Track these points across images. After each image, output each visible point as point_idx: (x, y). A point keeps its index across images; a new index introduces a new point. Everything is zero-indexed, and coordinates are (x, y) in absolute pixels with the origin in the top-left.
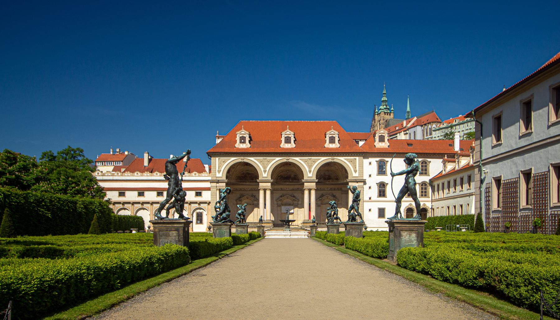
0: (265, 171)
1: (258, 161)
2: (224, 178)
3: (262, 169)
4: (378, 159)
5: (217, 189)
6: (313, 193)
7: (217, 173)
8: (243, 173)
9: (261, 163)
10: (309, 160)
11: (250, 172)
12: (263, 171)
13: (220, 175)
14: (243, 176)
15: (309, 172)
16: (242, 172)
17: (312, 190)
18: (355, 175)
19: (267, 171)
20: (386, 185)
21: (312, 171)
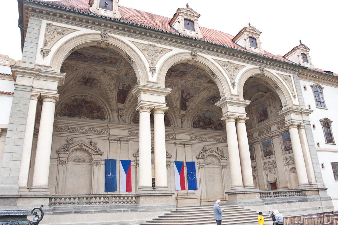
0: (153, 70)
1: (139, 47)
2: (57, 68)
3: (147, 66)
4: (313, 83)
5: (32, 96)
6: (242, 126)
7: (39, 56)
8: (76, 99)
9: (145, 52)
10: (229, 65)
11: (89, 100)
12: (148, 69)
13: (47, 61)
14: (75, 104)
15: (232, 85)
16: (74, 98)
17: (240, 121)
18: (296, 102)
19: (157, 70)
20: (330, 125)
21: (236, 84)
